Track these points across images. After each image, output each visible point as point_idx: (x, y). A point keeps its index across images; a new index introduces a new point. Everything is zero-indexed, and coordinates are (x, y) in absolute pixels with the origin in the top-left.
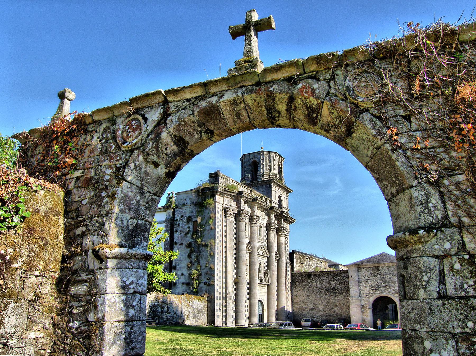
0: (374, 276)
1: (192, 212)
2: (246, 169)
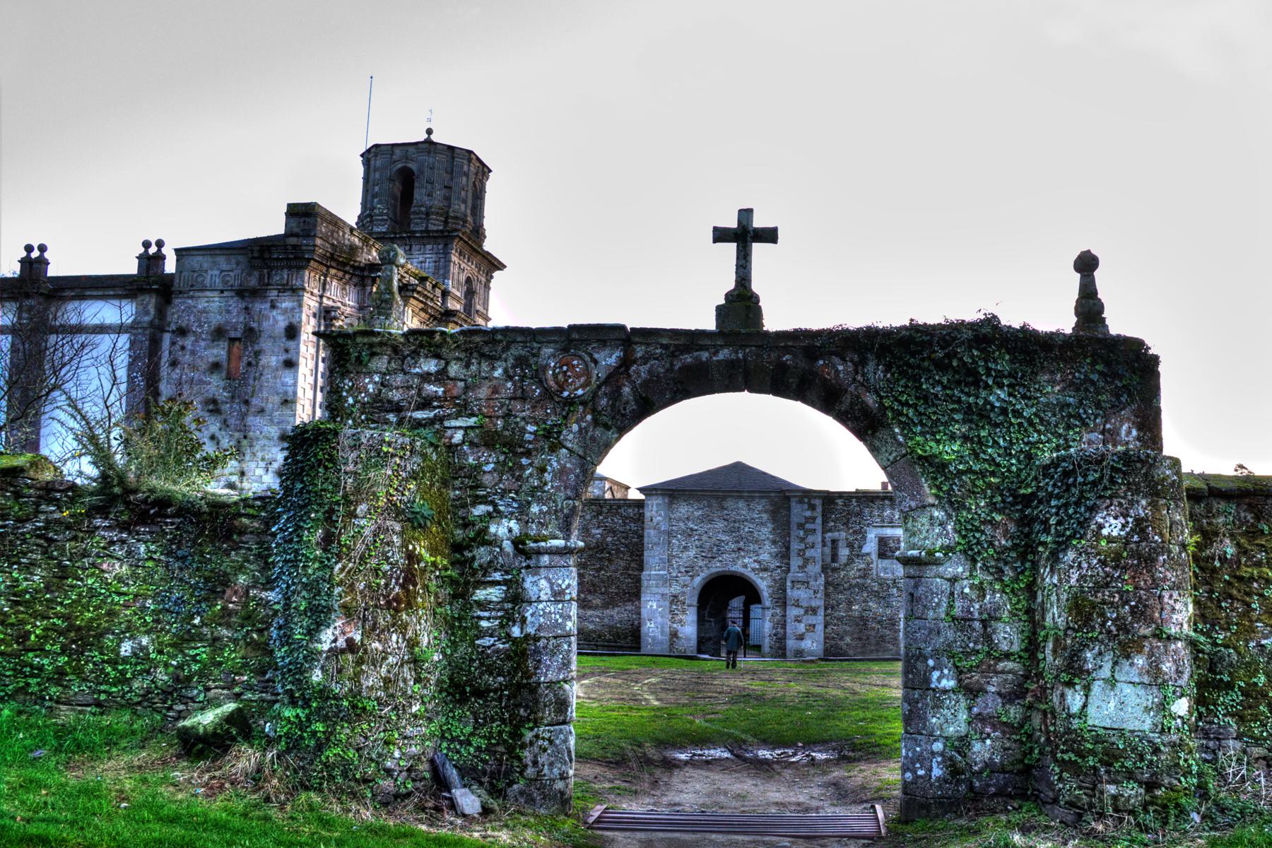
0: (711, 521)
1: (228, 312)
2: (377, 189)
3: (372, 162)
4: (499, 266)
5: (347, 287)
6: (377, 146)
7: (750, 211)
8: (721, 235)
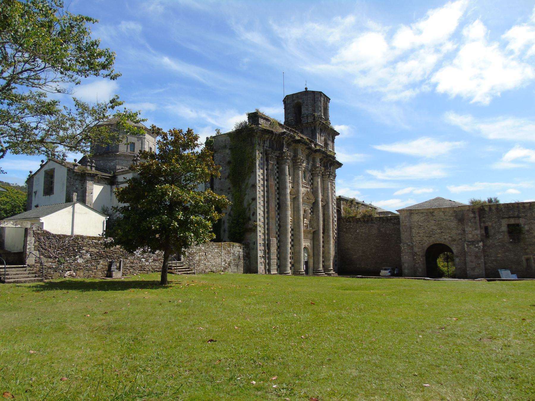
0: (428, 221)
3: (287, 102)
4: (338, 134)
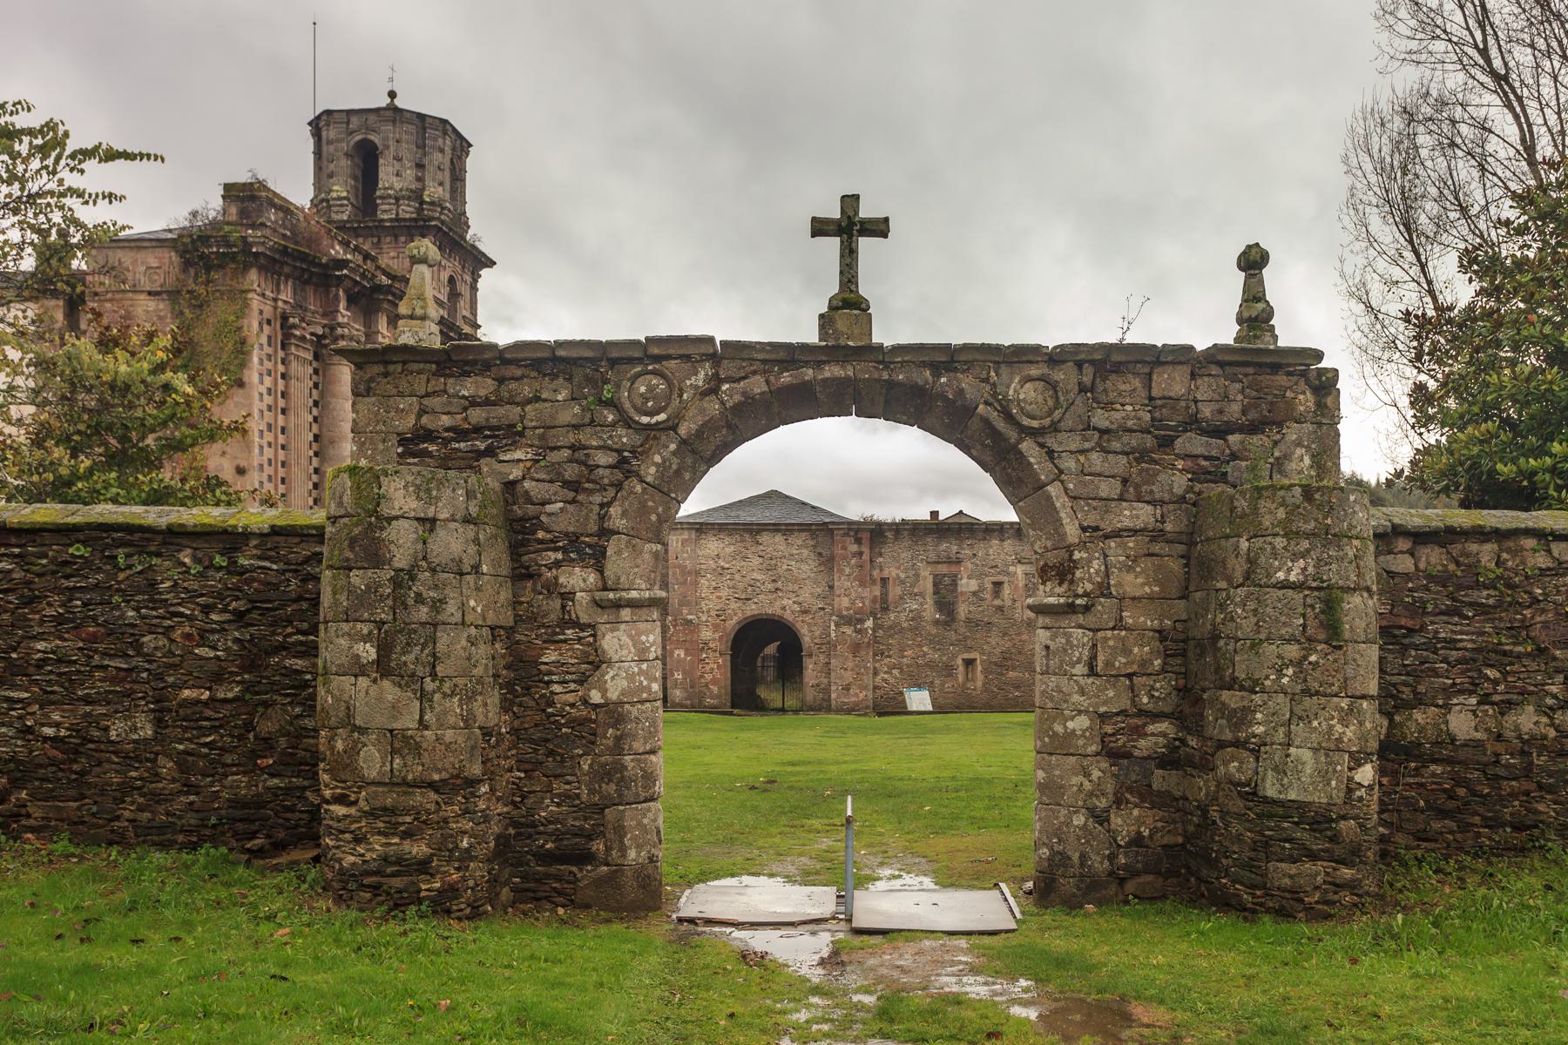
0: (745, 558)
2: (332, 167)
3: (324, 134)
4: (491, 263)
5: (307, 288)
6: (328, 113)
7: (856, 198)
8: (820, 228)
